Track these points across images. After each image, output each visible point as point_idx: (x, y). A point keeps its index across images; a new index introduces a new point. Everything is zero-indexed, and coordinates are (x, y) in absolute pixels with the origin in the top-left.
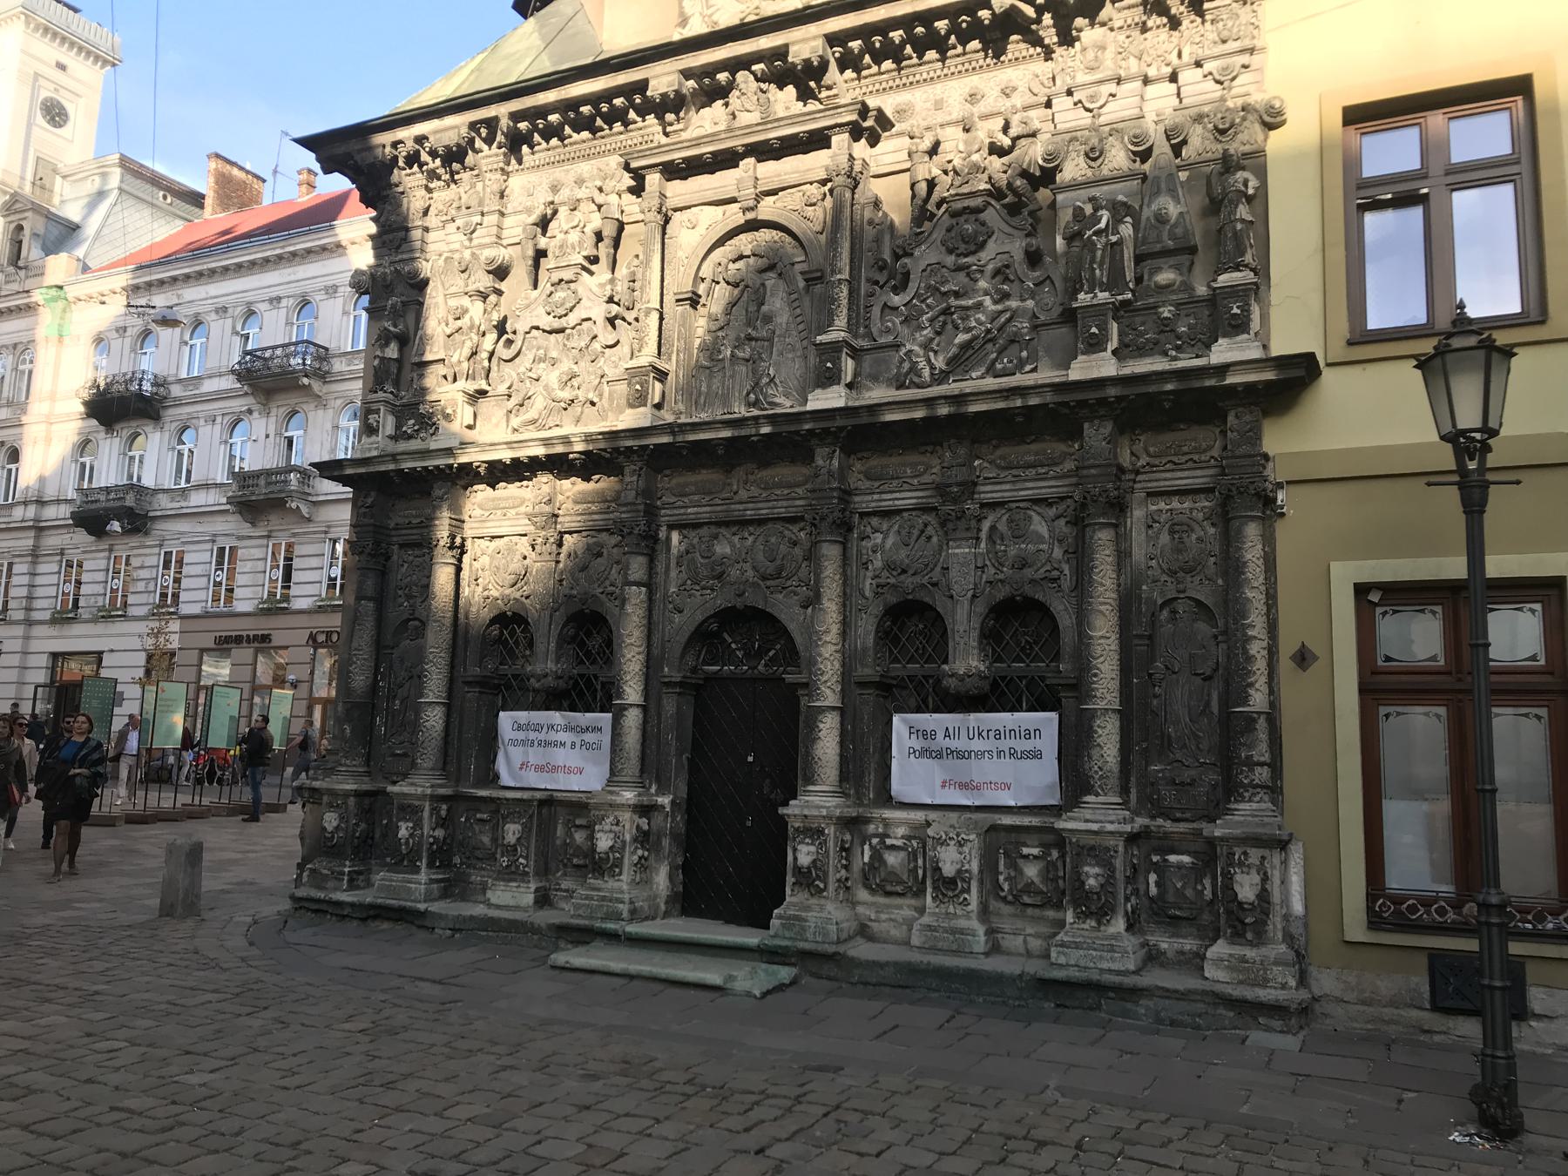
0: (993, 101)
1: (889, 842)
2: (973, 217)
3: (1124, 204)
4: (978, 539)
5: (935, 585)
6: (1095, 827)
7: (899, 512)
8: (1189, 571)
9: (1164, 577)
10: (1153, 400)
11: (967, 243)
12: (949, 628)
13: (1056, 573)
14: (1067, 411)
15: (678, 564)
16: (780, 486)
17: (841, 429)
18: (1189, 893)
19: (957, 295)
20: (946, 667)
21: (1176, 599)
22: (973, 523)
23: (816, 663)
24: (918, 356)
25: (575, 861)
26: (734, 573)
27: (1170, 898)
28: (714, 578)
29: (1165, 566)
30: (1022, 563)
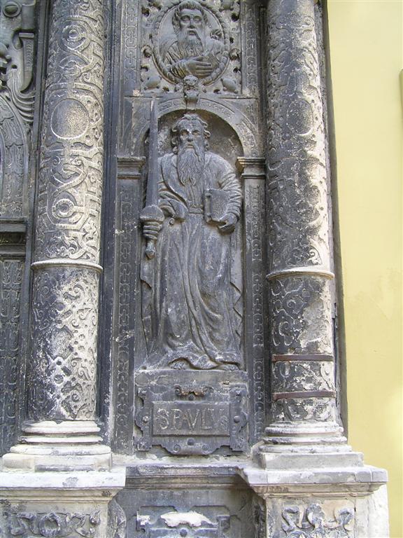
6: (56, 480)
9: (164, 83)
21: (180, 114)
29: (166, 66)
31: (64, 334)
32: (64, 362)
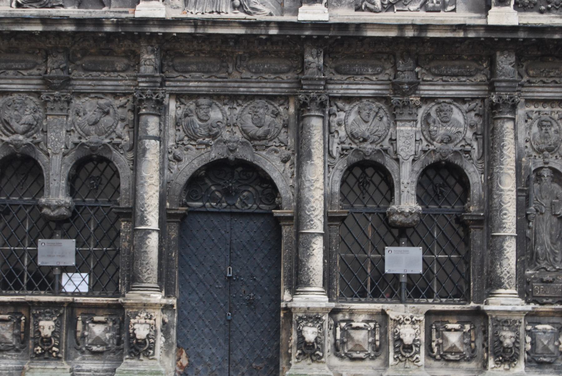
1: (354, 325)
4: (416, 121)
5: (386, 151)
6: (509, 308)
7: (360, 98)
8: (550, 150)
9: (534, 154)
10: (541, 44)
12: (395, 180)
13: (468, 148)
15: (177, 124)
16: (268, 71)
17: (331, 37)
18: (551, 347)
20: (394, 207)
21: (541, 168)
22: (414, 110)
23: (309, 202)
25: (95, 348)
26: (226, 135)
27: (539, 350)
28: (209, 136)
29: (535, 147)
30: (450, 140)
31: (507, 260)
32: (508, 269)
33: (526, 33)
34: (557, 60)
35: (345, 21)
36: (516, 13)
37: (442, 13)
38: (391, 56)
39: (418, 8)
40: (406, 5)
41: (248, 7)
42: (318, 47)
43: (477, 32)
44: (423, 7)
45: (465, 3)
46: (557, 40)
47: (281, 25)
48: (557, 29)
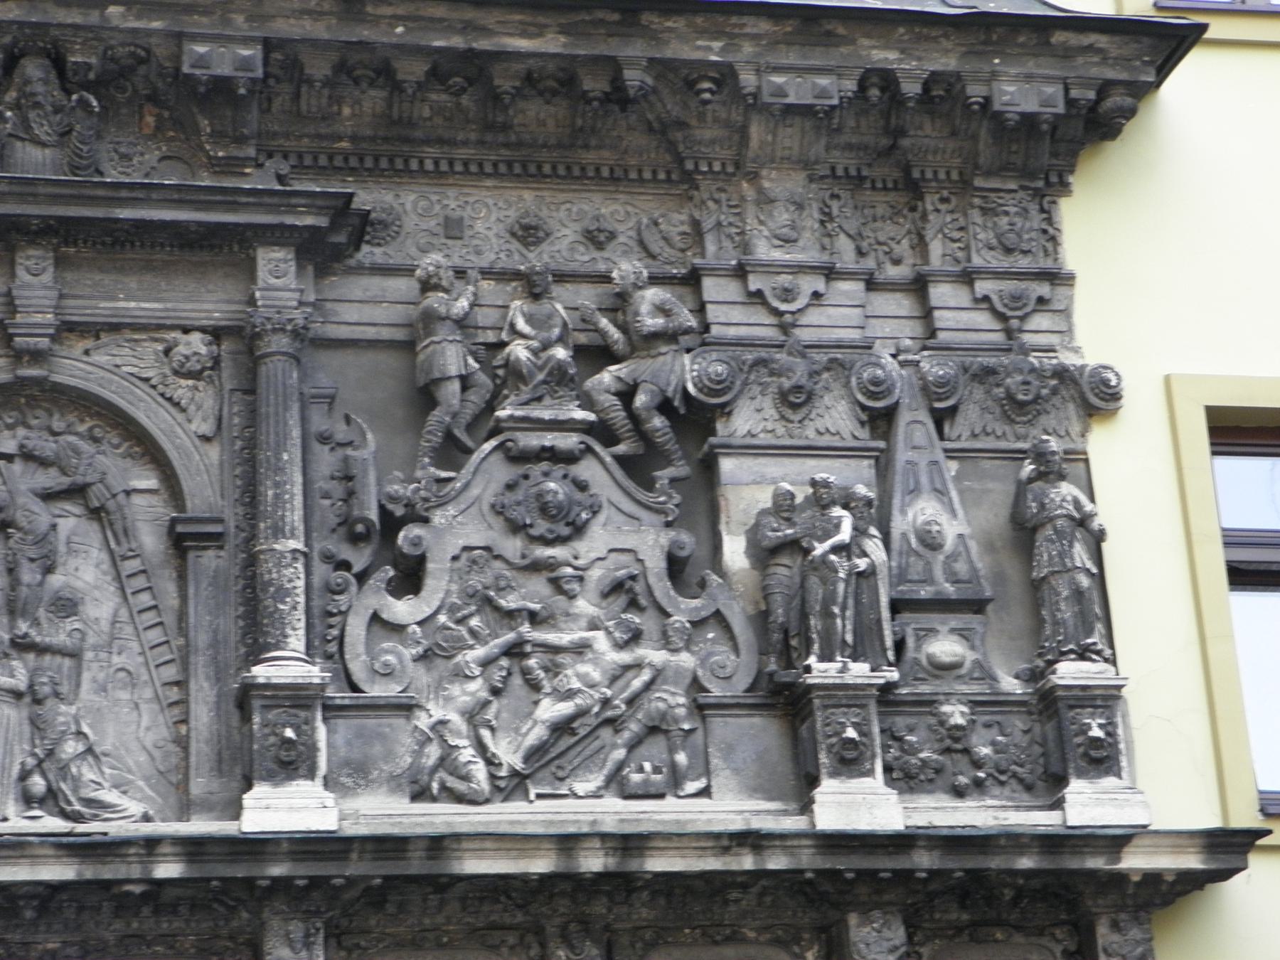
0: (563, 247)
2: (559, 470)
3: (869, 503)
11: (553, 519)
14: (827, 887)
17: (351, 882)
19: (534, 618)
24: (458, 734)
33: (936, 853)
34: (1019, 938)
35: (396, 831)
36: (893, 795)
37: (670, 802)
38: (530, 938)
39: (599, 788)
40: (562, 779)
41: (72, 799)
42: (308, 915)
43: (792, 855)
44: (614, 786)
45: (736, 771)
46: (1028, 874)
47: (194, 847)
48: (1025, 840)
